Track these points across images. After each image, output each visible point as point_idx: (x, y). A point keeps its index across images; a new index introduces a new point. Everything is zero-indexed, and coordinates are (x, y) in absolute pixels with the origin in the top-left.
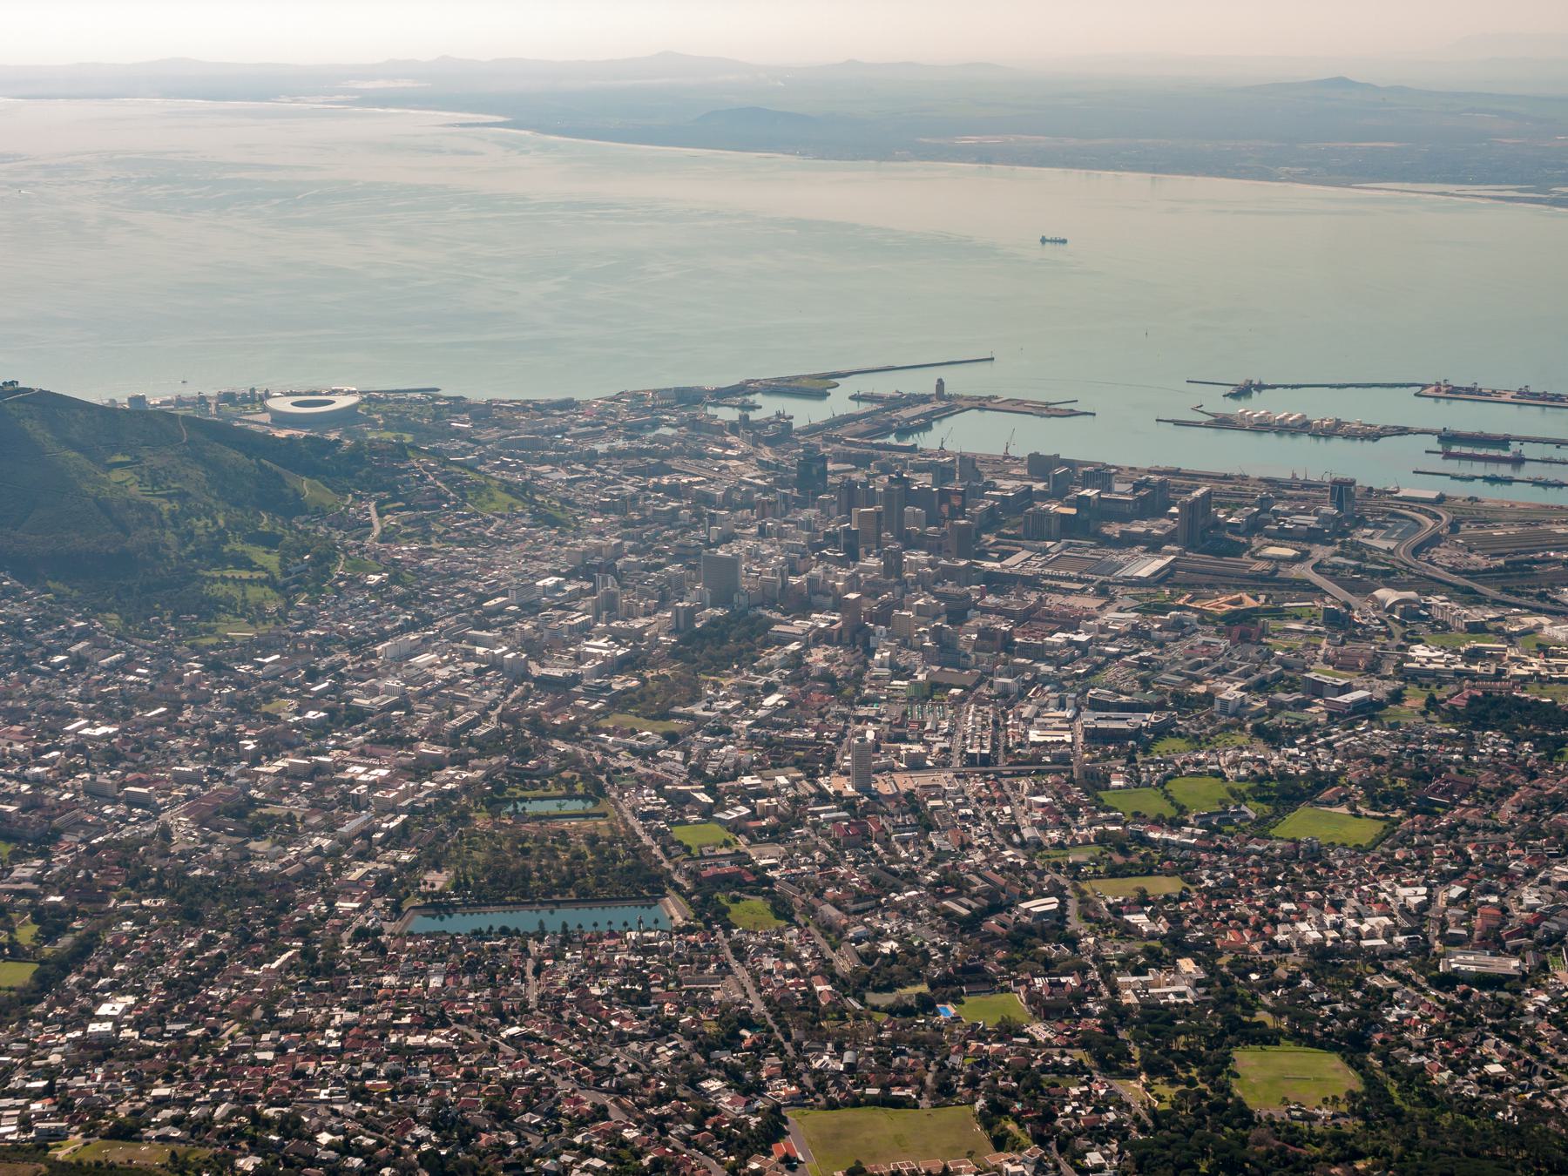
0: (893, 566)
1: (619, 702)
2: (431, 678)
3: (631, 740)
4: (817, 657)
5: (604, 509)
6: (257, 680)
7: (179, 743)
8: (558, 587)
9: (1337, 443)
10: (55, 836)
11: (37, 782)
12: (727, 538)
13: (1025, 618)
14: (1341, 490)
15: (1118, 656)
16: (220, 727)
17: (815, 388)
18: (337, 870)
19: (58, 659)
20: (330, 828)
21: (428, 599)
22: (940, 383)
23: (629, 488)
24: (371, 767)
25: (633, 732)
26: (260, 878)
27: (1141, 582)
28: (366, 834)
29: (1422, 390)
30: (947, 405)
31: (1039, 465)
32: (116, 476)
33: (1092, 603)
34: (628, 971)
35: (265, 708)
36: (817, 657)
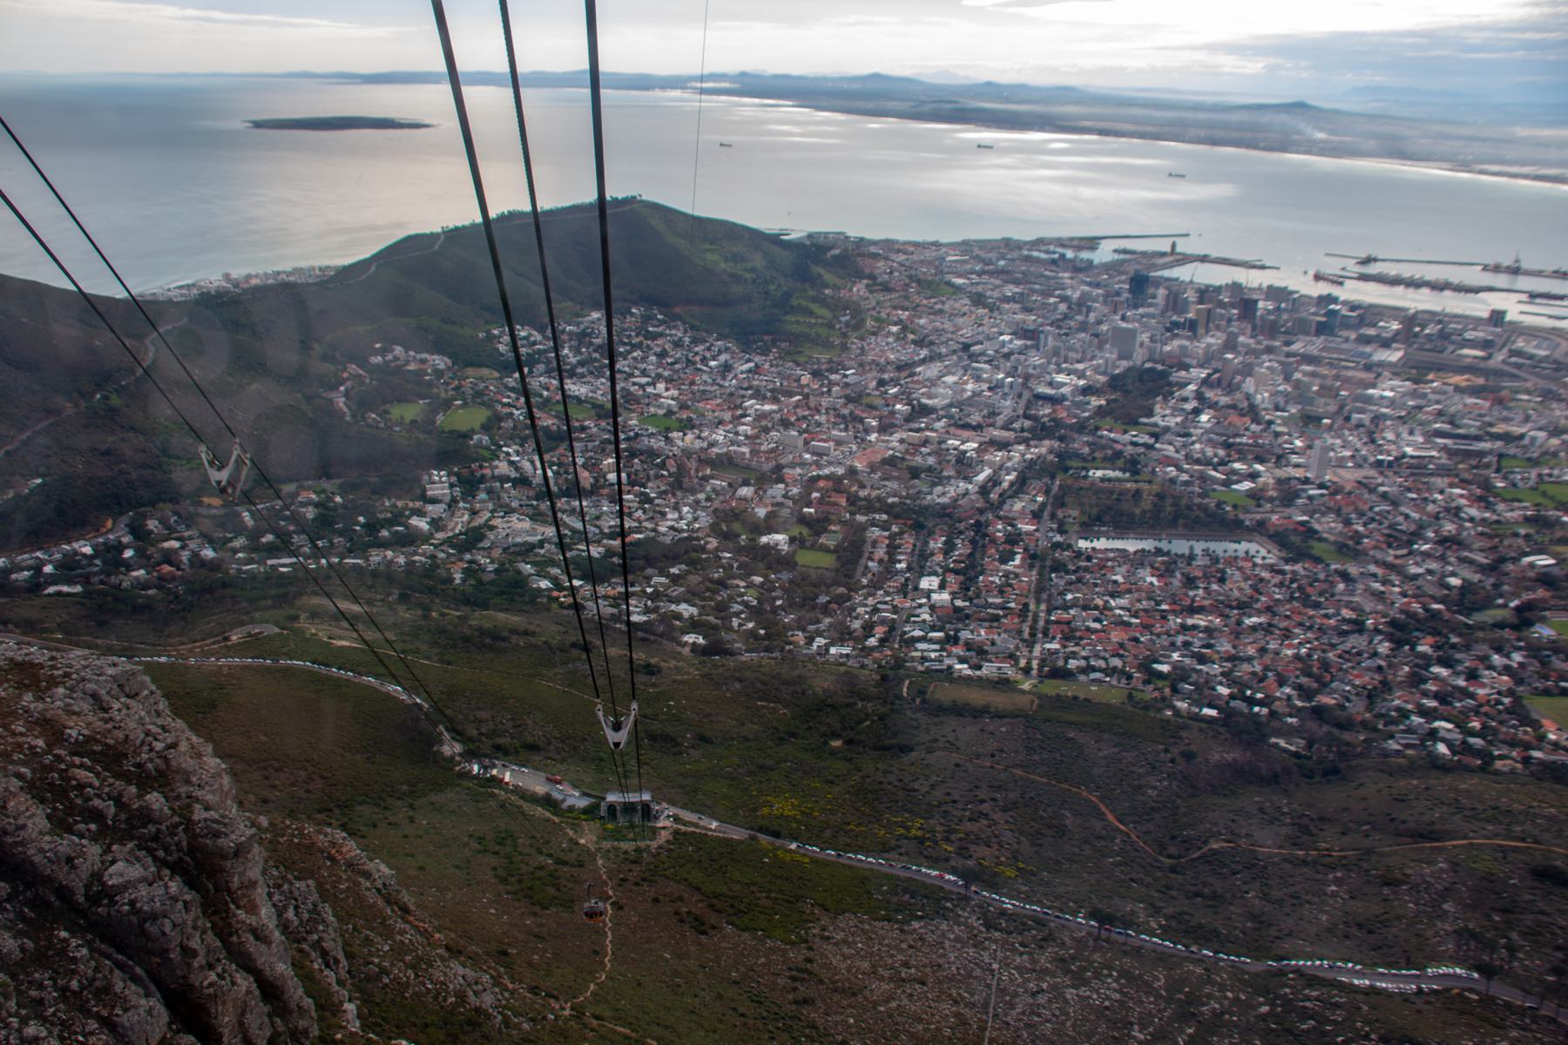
0: (1230, 345)
1: (1100, 412)
2: (964, 390)
3: (1127, 437)
4: (1209, 394)
5: (1007, 300)
6: (847, 385)
7: (822, 418)
8: (1011, 341)
9: (1447, 293)
10: (779, 468)
11: (747, 437)
12: (1099, 323)
13: (1337, 377)
14: (1497, 317)
15: (1419, 408)
16: (846, 412)
17: (1092, 243)
18: (996, 507)
19: (713, 363)
20: (967, 479)
21: (932, 343)
22: (1174, 246)
23: (1010, 290)
24: (963, 443)
25: (1125, 432)
26: (944, 507)
27: (1391, 365)
28: (994, 481)
29: (1486, 268)
30: (1186, 259)
31: (1275, 293)
32: (709, 256)
33: (1372, 376)
34: (1281, 585)
35: (865, 401)
36: (1209, 394)
